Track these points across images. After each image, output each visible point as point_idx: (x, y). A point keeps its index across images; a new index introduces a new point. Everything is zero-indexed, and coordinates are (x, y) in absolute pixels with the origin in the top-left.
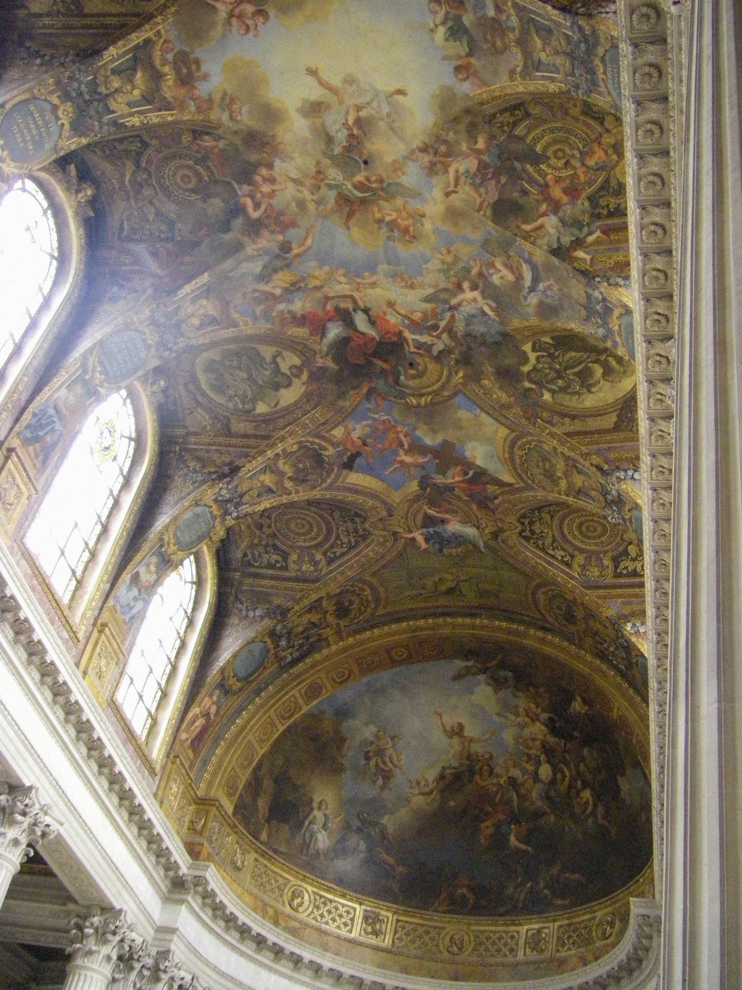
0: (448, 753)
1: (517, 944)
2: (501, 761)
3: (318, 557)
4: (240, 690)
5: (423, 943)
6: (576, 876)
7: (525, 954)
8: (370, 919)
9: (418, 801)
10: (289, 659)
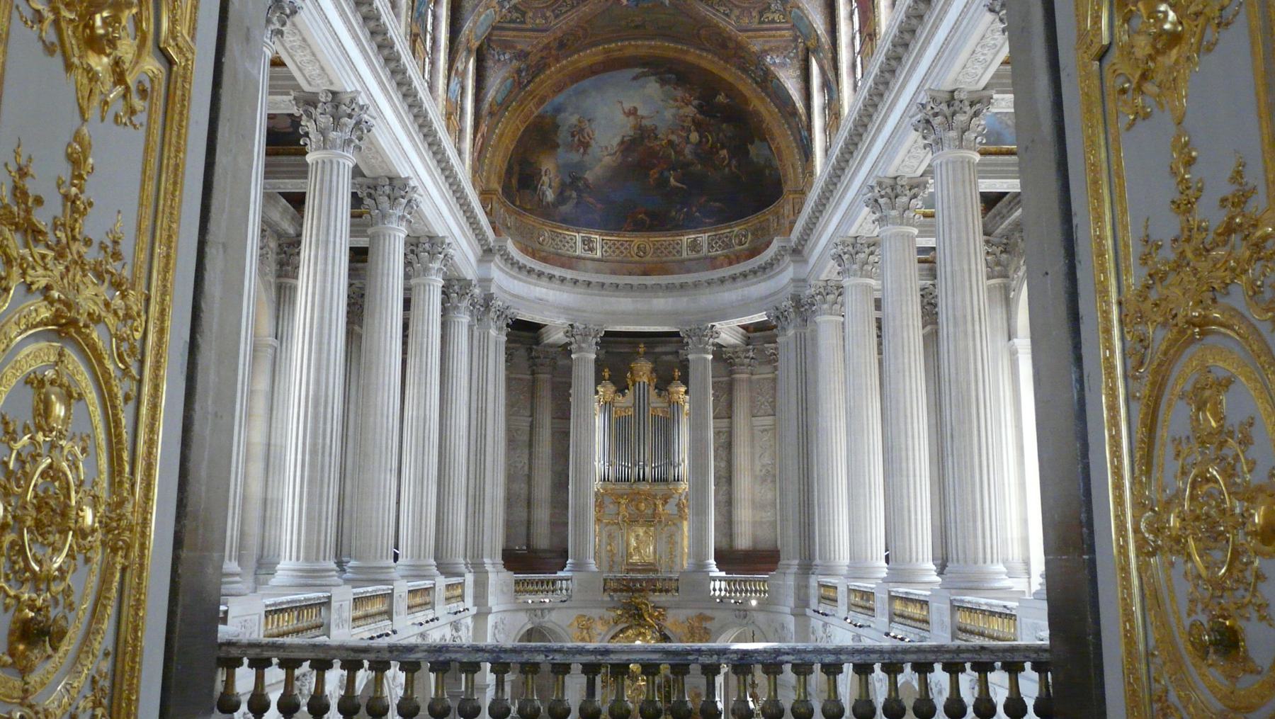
6: (717, 204)
8: (587, 242)
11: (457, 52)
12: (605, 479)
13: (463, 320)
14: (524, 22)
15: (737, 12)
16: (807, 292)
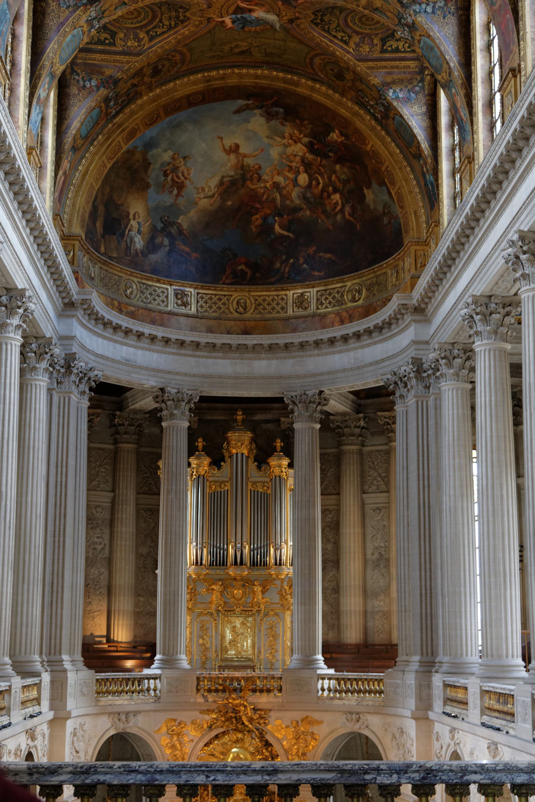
0: (227, 165)
1: (286, 304)
2: (268, 169)
3: (142, 35)
4: (82, 145)
5: (218, 308)
6: (328, 255)
7: (293, 311)
8: (180, 295)
9: (204, 203)
10: (114, 111)
11: (39, 77)
12: (198, 563)
13: (41, 382)
14: (114, 44)
15: (356, 39)
16: (432, 356)
